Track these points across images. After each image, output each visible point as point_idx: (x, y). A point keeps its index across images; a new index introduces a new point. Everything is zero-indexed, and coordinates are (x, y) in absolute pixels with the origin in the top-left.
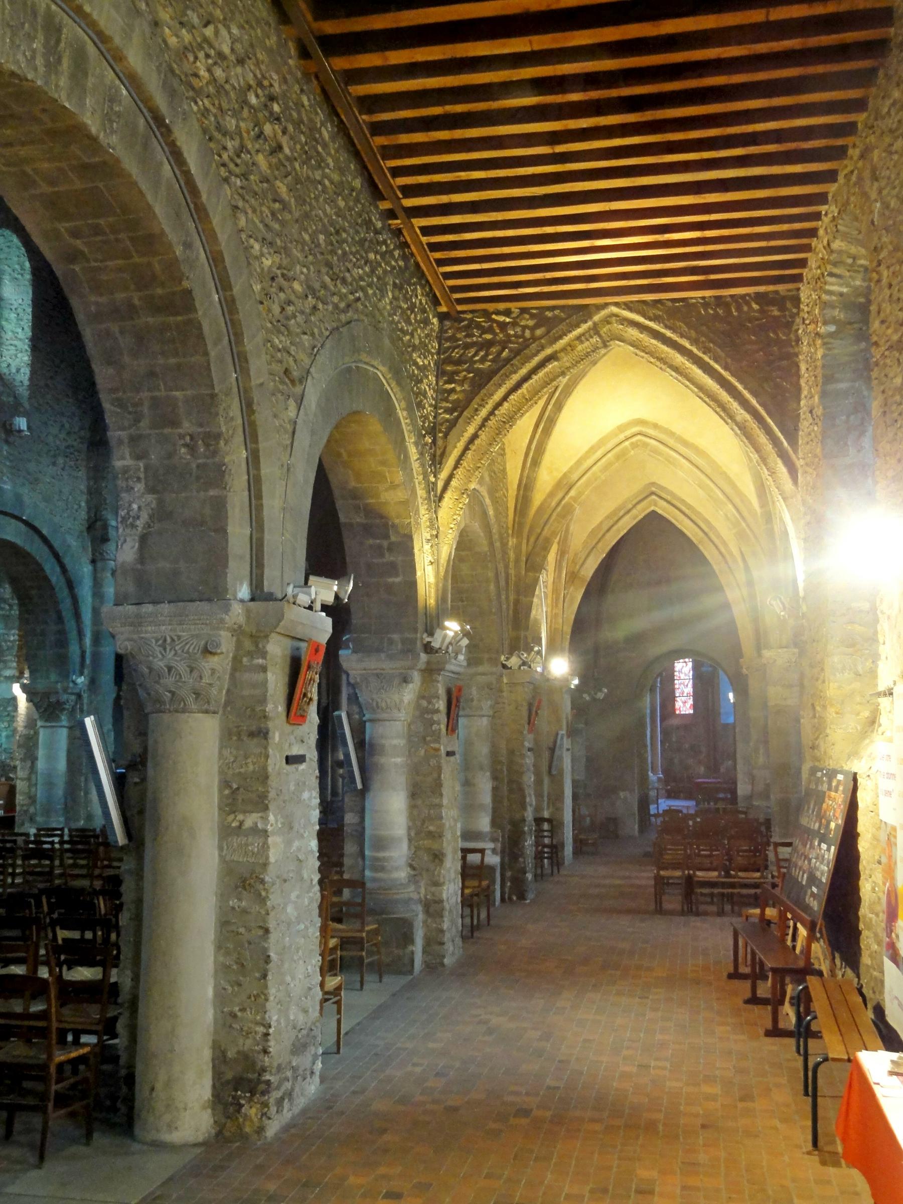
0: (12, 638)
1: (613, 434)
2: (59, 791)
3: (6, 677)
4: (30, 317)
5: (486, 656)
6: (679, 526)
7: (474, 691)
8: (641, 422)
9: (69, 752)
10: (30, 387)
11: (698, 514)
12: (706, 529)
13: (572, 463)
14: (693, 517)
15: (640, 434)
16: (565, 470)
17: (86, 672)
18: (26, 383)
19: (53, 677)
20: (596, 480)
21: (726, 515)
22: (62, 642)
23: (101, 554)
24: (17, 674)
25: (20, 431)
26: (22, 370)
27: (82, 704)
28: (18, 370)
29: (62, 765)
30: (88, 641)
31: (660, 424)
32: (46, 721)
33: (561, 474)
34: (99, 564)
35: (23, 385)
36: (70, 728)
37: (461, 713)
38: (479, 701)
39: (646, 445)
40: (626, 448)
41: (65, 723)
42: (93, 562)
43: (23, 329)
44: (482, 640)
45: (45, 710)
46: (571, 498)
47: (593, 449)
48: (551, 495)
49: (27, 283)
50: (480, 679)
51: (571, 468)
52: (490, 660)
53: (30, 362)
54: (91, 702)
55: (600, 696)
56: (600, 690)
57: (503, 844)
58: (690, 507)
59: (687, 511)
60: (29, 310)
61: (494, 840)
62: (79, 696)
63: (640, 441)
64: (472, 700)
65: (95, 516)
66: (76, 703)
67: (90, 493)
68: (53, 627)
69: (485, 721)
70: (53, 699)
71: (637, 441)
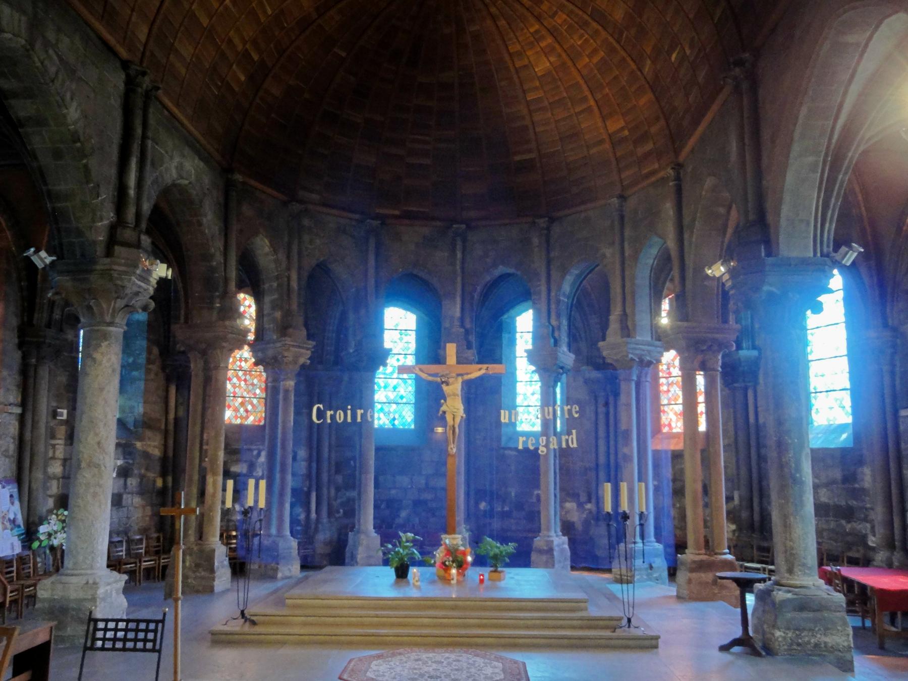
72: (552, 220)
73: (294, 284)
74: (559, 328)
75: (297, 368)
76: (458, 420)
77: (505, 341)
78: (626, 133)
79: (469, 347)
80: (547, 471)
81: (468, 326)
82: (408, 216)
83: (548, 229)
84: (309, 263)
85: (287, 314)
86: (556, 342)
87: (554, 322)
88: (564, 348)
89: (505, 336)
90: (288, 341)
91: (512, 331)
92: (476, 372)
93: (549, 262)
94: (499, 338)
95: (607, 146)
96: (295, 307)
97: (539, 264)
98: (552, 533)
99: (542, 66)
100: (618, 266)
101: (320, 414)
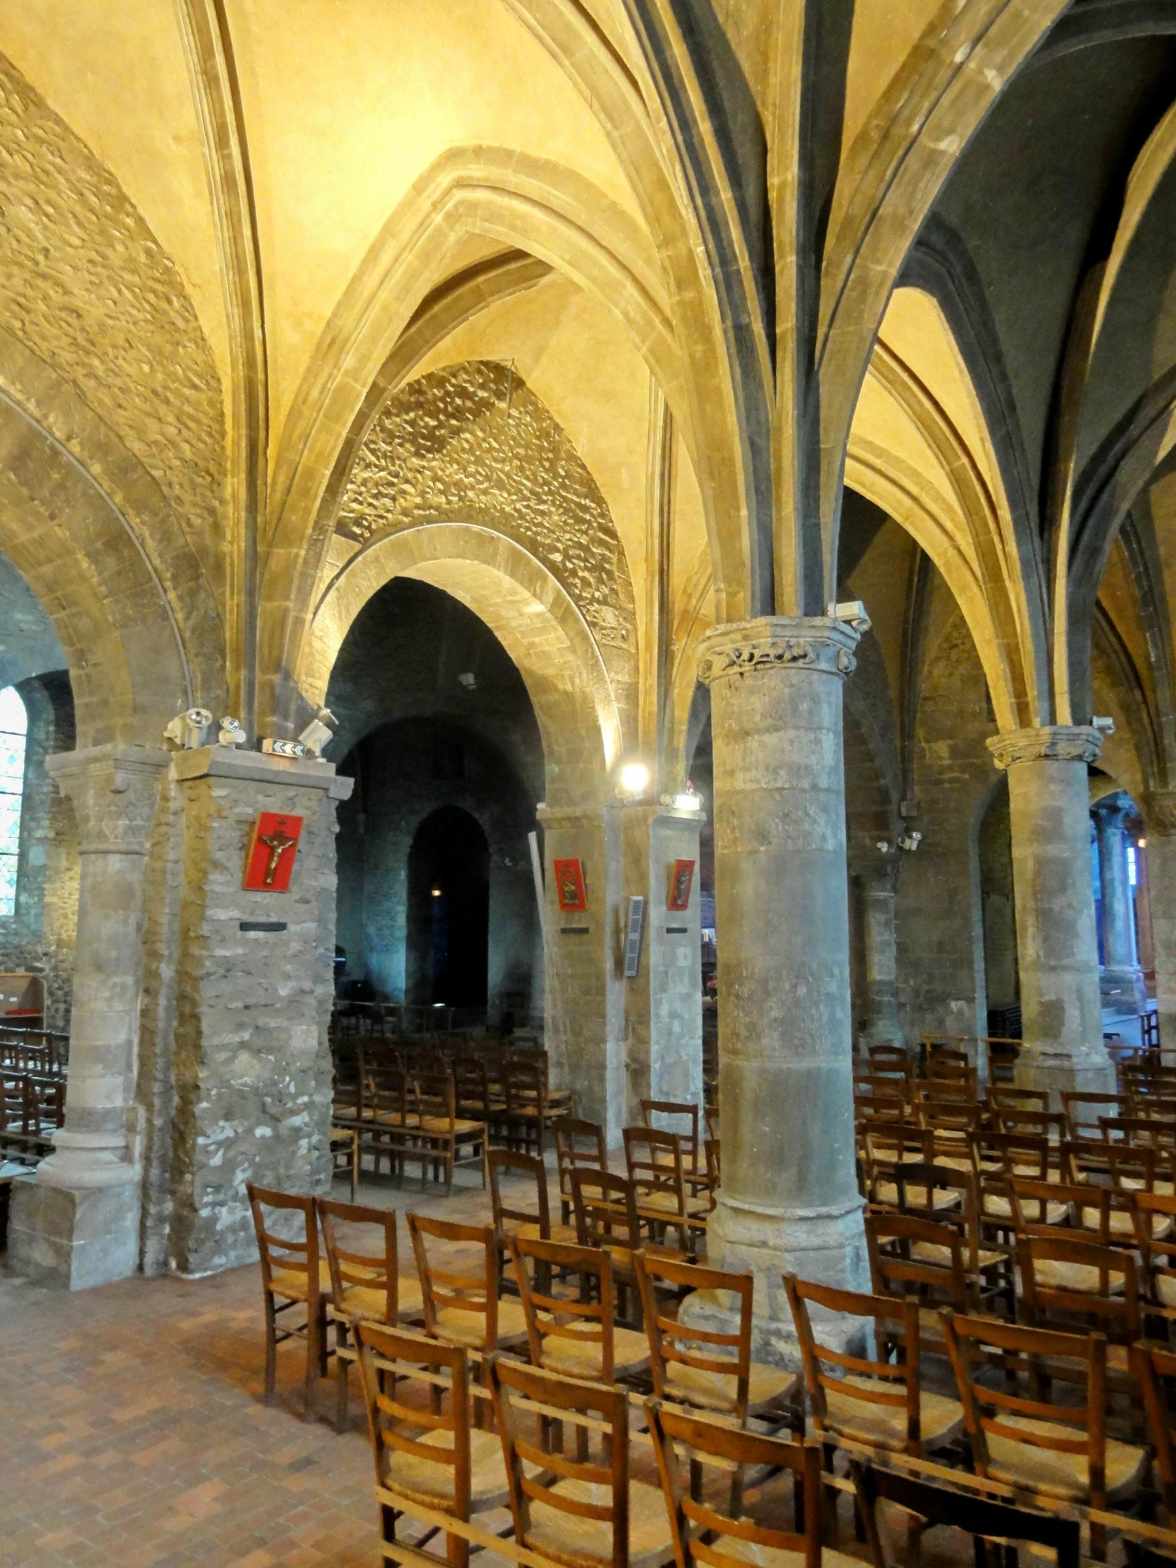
0: (45, 789)
1: (408, 204)
3: (38, 839)
6: (869, 496)
8: (454, 155)
11: (898, 462)
12: (915, 490)
13: (338, 294)
14: (892, 473)
15: (462, 184)
16: (328, 314)
20: (390, 319)
21: (626, 315)
24: (52, 835)
31: (485, 143)
33: (323, 324)
39: (473, 206)
40: (438, 230)
46: (347, 372)
47: (374, 252)
48: (311, 372)
51: (339, 305)
55: (912, 844)
56: (911, 837)
58: (881, 453)
59: (878, 463)
63: (461, 203)
71: (456, 206)
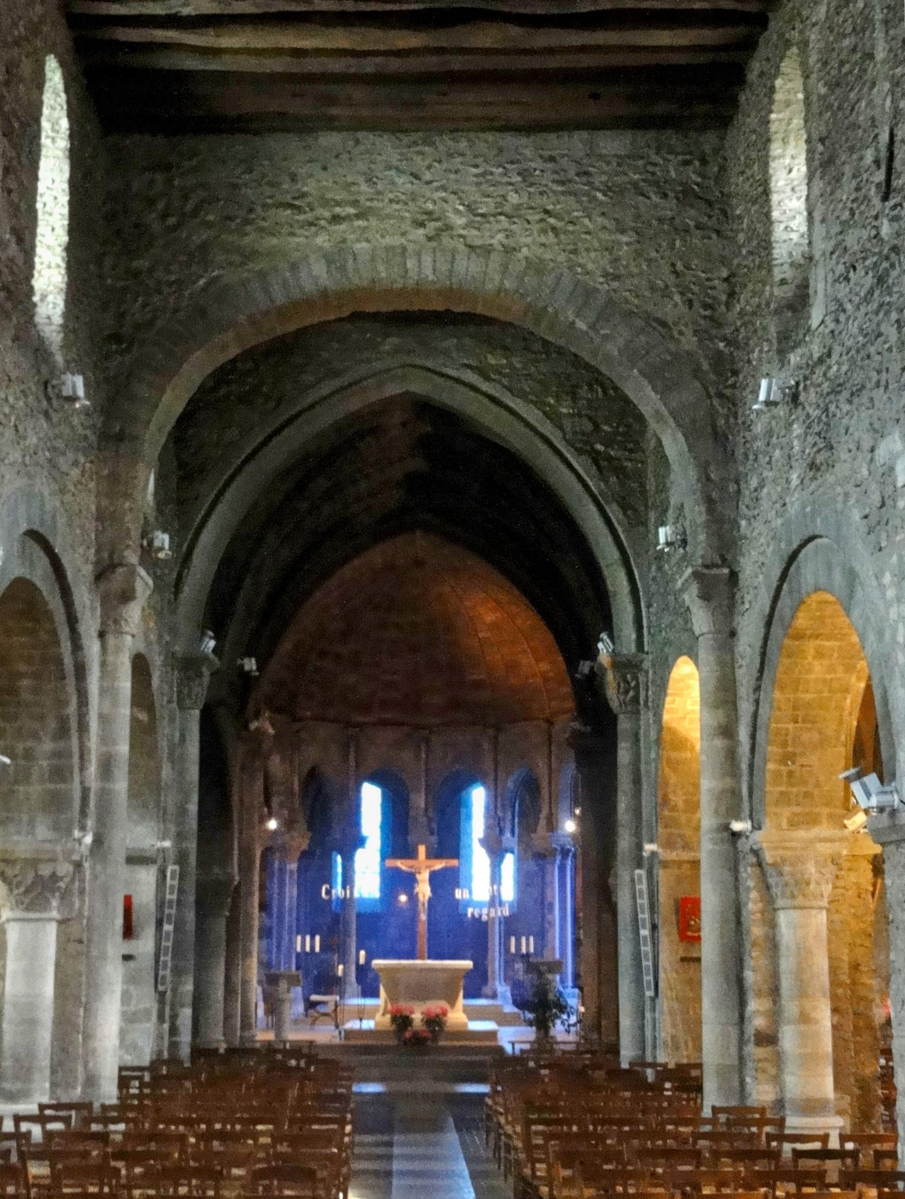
2: (45, 1037)
4: (66, 211)
5: (825, 811)
7: (811, 869)
9: (58, 965)
10: (65, 327)
17: (90, 823)
18: (58, 320)
19: (43, 831)
22: (60, 773)
23: (116, 622)
25: (73, 399)
26: (50, 298)
27: (82, 881)
28: (44, 297)
29: (48, 989)
30: (93, 769)
32: (27, 909)
34: (111, 640)
35: (51, 324)
36: (61, 923)
37: (780, 903)
38: (818, 884)
41: (55, 914)
42: (102, 635)
43: (53, 229)
44: (818, 785)
45: (27, 891)
49: (60, 154)
50: (825, 848)
52: (830, 816)
53: (64, 286)
54: (95, 877)
57: (853, 1117)
60: (65, 199)
61: (840, 1113)
62: (78, 865)
64: (808, 883)
65: (111, 555)
66: (73, 880)
67: (100, 516)
68: (48, 746)
69: (823, 917)
70: (45, 871)
72: (498, 729)
73: (296, 787)
74: (504, 819)
75: (298, 854)
76: (427, 898)
77: (463, 817)
78: (551, 674)
79: (432, 833)
80: (494, 935)
81: (431, 815)
82: (384, 723)
83: (496, 737)
84: (306, 768)
85: (292, 811)
86: (501, 832)
87: (500, 814)
88: (508, 834)
89: (463, 811)
90: (295, 834)
91: (468, 806)
92: (439, 865)
93: (496, 763)
94: (457, 813)
95: (539, 680)
96: (297, 806)
97: (488, 765)
98: (497, 983)
99: (490, 618)
100: (546, 777)
101: (328, 892)
